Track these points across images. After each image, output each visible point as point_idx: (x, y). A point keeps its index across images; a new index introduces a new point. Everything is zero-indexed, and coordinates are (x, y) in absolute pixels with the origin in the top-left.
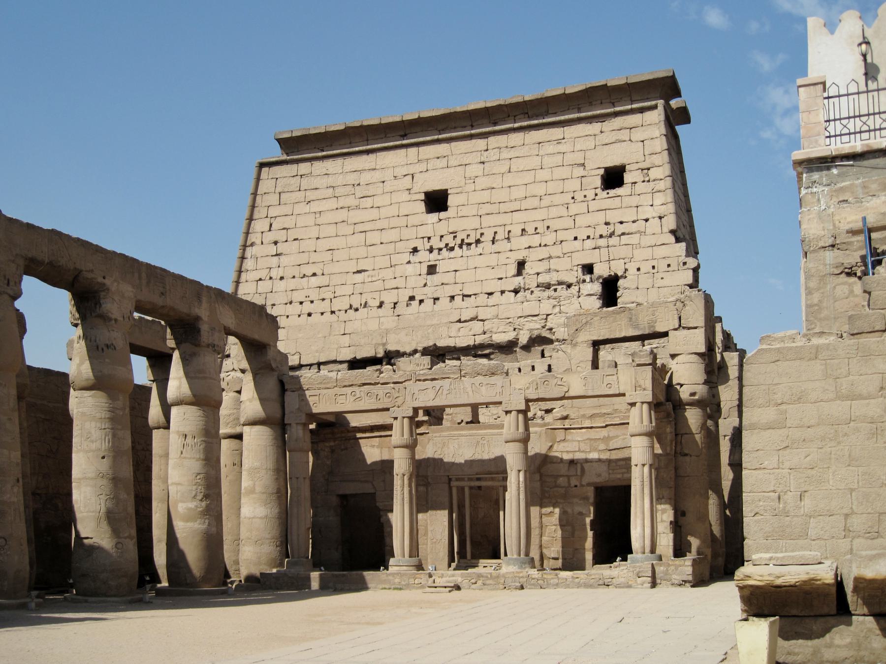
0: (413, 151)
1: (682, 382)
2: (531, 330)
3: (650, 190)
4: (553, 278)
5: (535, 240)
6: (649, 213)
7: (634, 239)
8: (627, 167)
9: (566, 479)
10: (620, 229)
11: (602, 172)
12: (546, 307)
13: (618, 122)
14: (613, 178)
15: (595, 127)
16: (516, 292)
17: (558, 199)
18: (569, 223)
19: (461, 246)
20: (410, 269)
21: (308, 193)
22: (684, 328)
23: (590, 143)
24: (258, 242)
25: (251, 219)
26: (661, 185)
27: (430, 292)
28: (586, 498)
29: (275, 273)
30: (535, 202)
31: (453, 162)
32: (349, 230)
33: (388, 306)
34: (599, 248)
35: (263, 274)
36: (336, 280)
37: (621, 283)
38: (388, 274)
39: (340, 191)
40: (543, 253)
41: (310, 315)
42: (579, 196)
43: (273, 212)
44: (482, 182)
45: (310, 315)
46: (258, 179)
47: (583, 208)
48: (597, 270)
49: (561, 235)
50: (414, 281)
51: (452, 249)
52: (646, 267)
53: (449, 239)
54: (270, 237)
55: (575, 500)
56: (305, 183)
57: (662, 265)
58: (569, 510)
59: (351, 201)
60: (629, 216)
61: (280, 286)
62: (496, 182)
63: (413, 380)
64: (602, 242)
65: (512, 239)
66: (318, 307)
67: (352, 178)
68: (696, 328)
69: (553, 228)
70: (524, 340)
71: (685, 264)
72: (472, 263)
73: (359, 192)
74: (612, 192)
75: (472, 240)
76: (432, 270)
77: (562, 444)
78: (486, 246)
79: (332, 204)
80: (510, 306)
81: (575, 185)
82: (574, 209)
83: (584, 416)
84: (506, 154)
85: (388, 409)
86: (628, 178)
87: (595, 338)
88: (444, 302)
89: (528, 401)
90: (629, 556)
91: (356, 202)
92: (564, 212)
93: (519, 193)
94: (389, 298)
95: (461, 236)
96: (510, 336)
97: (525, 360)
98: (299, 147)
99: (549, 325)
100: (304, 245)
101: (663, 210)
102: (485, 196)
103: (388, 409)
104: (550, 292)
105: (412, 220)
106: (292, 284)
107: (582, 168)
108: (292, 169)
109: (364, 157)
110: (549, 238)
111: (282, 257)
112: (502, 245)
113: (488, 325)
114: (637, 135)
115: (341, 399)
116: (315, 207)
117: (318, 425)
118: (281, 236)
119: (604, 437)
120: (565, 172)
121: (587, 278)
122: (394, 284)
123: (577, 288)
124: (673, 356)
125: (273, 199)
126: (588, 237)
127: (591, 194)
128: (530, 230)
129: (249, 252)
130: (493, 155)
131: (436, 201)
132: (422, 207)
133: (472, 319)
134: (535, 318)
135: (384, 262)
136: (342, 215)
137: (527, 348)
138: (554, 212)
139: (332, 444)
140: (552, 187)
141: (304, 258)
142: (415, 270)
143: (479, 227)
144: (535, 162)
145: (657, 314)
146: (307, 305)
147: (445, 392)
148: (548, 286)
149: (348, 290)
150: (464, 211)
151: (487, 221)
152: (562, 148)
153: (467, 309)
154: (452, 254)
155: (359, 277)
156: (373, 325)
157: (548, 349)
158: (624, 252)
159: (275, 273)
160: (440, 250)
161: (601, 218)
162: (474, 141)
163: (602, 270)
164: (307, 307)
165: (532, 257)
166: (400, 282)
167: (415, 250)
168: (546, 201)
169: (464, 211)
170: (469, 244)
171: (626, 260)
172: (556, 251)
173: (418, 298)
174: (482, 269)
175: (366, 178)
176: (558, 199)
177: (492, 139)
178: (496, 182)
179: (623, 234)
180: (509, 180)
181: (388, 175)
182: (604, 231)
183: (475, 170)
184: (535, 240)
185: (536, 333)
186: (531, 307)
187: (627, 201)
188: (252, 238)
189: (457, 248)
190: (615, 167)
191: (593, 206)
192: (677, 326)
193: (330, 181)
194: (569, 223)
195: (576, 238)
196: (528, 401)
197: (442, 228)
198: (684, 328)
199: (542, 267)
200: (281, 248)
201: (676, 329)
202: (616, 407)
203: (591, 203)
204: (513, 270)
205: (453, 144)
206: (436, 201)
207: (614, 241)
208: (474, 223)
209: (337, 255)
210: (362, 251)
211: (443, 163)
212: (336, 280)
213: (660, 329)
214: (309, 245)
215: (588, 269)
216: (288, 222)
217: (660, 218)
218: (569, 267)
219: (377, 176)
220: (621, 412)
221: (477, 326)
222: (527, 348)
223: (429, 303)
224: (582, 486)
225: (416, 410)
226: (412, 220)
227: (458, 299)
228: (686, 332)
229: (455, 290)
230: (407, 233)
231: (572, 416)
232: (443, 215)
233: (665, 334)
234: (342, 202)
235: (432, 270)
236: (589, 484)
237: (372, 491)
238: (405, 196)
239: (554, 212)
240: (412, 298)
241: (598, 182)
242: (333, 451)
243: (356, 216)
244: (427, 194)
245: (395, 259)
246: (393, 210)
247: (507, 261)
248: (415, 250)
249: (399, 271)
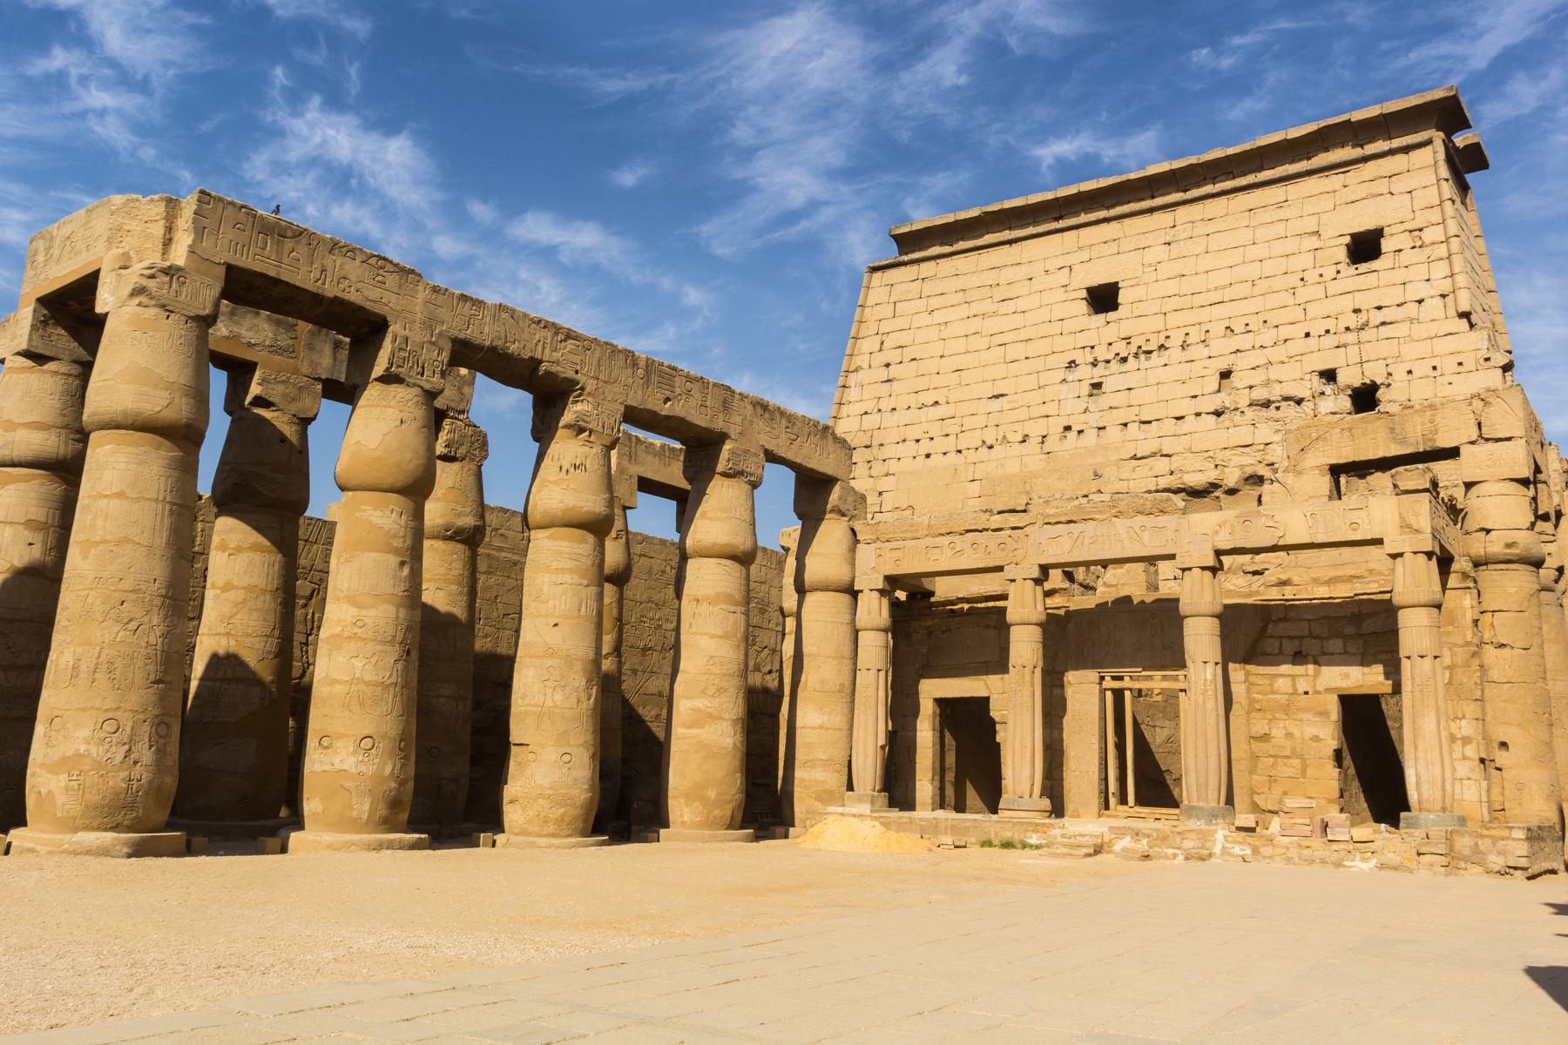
1: (1488, 527)
2: (1242, 467)
3: (1424, 259)
5: (1244, 342)
6: (1423, 291)
7: (1400, 330)
8: (1386, 231)
9: (1289, 680)
11: (1347, 239)
12: (1264, 433)
13: (1371, 168)
14: (1365, 247)
16: (1218, 414)
18: (1298, 314)
19: (1136, 356)
21: (931, 300)
22: (1487, 440)
23: (1327, 203)
24: (865, 365)
27: (1094, 419)
28: (1324, 714)
29: (884, 405)
30: (1244, 289)
31: (1125, 246)
33: (1034, 441)
34: (1345, 346)
35: (868, 406)
36: (965, 409)
37: (1380, 394)
38: (1036, 397)
40: (1258, 358)
41: (928, 456)
42: (1312, 276)
43: (884, 328)
44: (1167, 269)
45: (928, 456)
47: (1319, 292)
48: (1343, 378)
49: (1285, 332)
51: (1124, 360)
52: (1421, 369)
55: (1305, 716)
56: (928, 288)
57: (1449, 365)
58: (1297, 733)
59: (987, 306)
61: (891, 420)
62: (1188, 266)
63: (1040, 523)
64: (1350, 338)
65: (1212, 343)
66: (940, 444)
67: (989, 278)
68: (1509, 439)
69: (1272, 322)
71: (1487, 359)
72: (1153, 377)
73: (999, 294)
74: (1363, 267)
75: (1153, 346)
77: (1282, 625)
78: (1174, 354)
79: (964, 311)
80: (1208, 433)
81: (1306, 261)
82: (1304, 294)
83: (1316, 581)
84: (1201, 229)
85: (1000, 569)
86: (1386, 245)
87: (1334, 461)
88: (1114, 433)
89: (1219, 553)
90: (1402, 815)
91: (995, 307)
92: (1289, 300)
93: (1223, 278)
94: (1035, 430)
95: (1135, 343)
99: (1270, 459)
100: (922, 367)
103: (1000, 569)
104: (1272, 412)
105: (1069, 325)
107: (1315, 238)
108: (910, 271)
111: (895, 384)
112: (1197, 352)
113: (1175, 463)
115: (934, 554)
116: (939, 317)
117: (910, 596)
119: (1353, 614)
120: (1291, 245)
121: (1328, 389)
122: (1043, 410)
123: (1311, 405)
124: (1469, 486)
125: (887, 310)
126: (1328, 332)
127: (1330, 272)
128: (1238, 327)
131: (1103, 299)
132: (1083, 307)
133: (1153, 455)
134: (1247, 450)
135: (1031, 382)
136: (975, 324)
138: (1273, 301)
139: (930, 623)
140: (1269, 267)
141: (922, 383)
143: (1161, 328)
144: (1245, 236)
145: (1438, 419)
146: (925, 443)
147: (1087, 541)
148: (1266, 404)
149: (980, 421)
151: (1174, 320)
154: (1126, 367)
156: (1013, 467)
158: (1387, 349)
159: (885, 405)
160: (1108, 362)
161: (1348, 303)
162: (1156, 215)
163: (1350, 377)
164: (925, 446)
165: (1241, 363)
166: (1051, 409)
167: (1072, 364)
168: (1262, 286)
169: (1141, 309)
170: (1150, 352)
171: (1389, 361)
172: (1275, 354)
173: (1075, 428)
175: (1009, 274)
177: (1181, 210)
178: (1188, 266)
179: (1383, 323)
180: (1206, 262)
181: (1037, 269)
182: (1353, 321)
184: (1244, 342)
185: (1249, 471)
187: (1386, 277)
189: (1131, 359)
190: (1369, 232)
191: (1334, 288)
192: (1474, 436)
195: (1307, 335)
196: (1219, 553)
197: (1112, 333)
198: (1487, 440)
199: (1256, 378)
200: (894, 371)
201: (1473, 443)
202: (1371, 566)
203: (1330, 285)
204: (1214, 382)
205: (1127, 221)
206: (1103, 299)
207: (1364, 335)
208: (1158, 323)
210: (1001, 370)
211: (1113, 247)
212: (965, 409)
213: (1445, 442)
215: (1329, 376)
216: (903, 338)
217: (1443, 296)
218: (1299, 375)
219: (1023, 272)
220: (1381, 574)
221: (1162, 465)
223: (1091, 435)
224: (1318, 692)
225: (1045, 569)
226: (1069, 325)
227: (1133, 427)
228: (1490, 445)
230: (1060, 343)
231: (1296, 579)
232: (1111, 315)
233: (1452, 453)
234: (975, 308)
236: (1328, 690)
237: (985, 694)
238: (1060, 295)
239: (1273, 301)
240: (1068, 428)
241: (1342, 254)
242: (930, 633)
244: (1089, 290)
245: (1045, 378)
246: (1044, 315)
247: (1205, 372)
248: (1072, 364)
249: (1049, 393)
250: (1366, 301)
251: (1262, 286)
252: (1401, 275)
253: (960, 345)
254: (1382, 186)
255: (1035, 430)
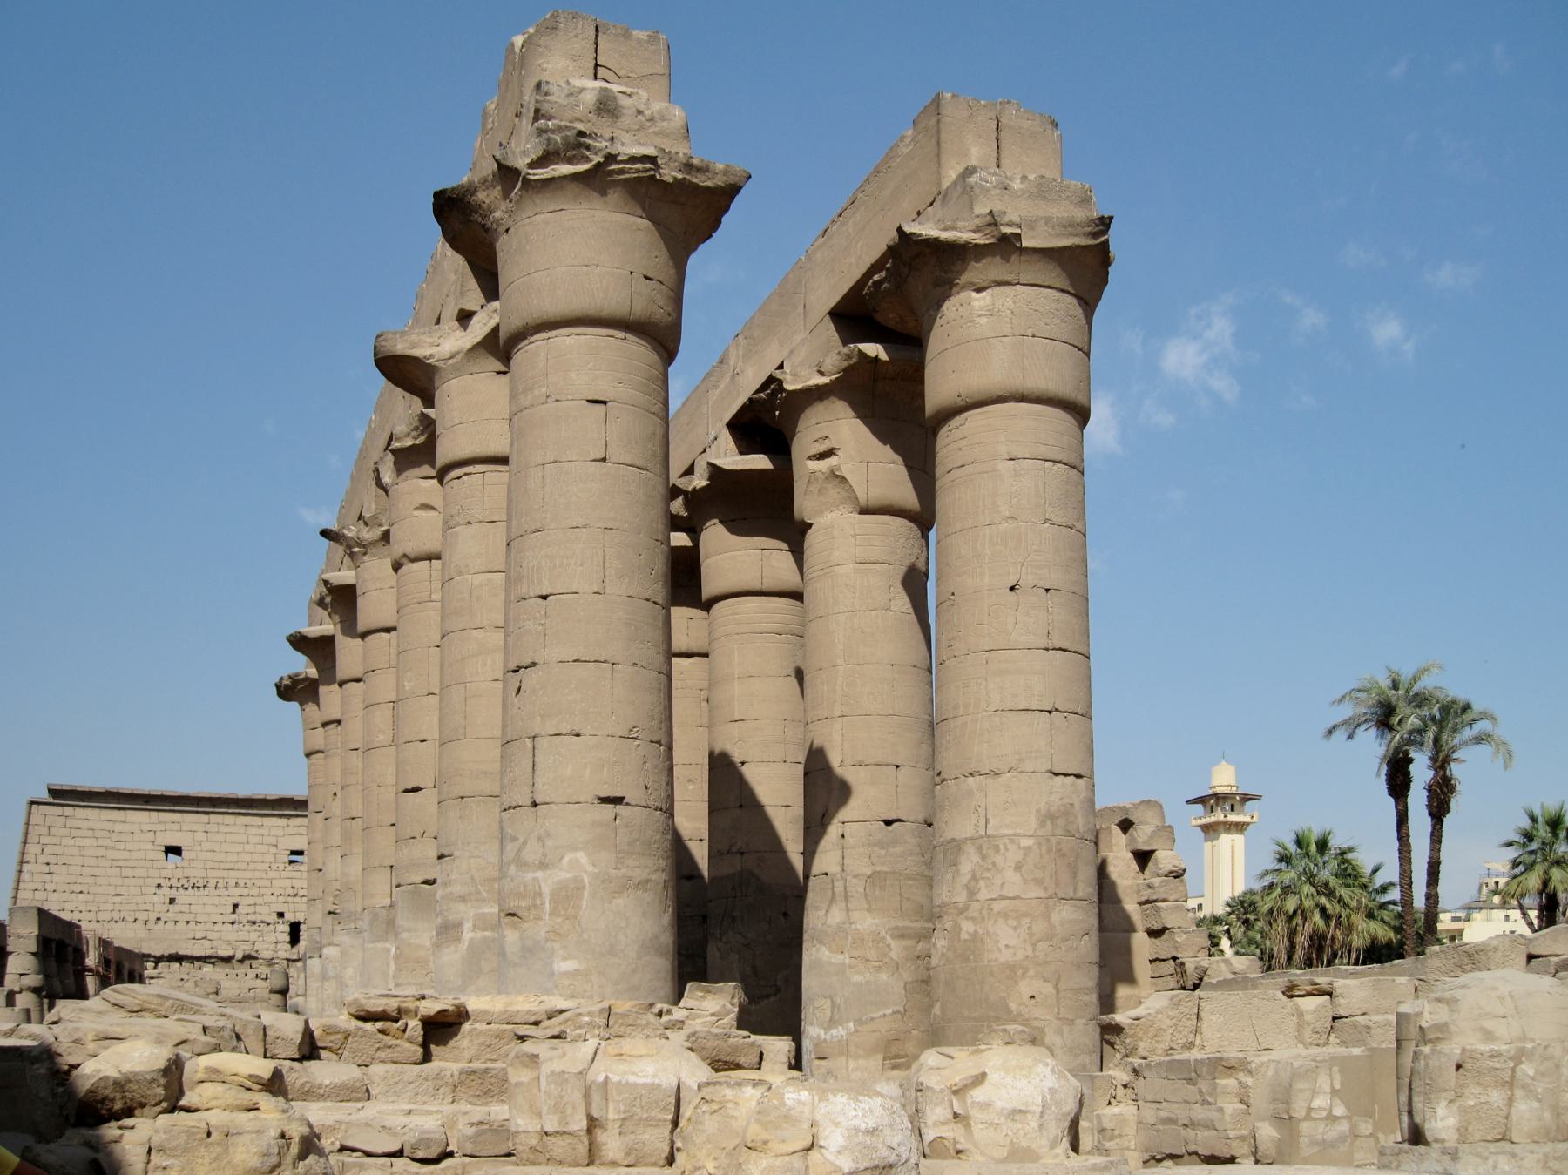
0: (154, 814)
4: (258, 918)
5: (245, 891)
12: (253, 936)
15: (284, 821)
17: (260, 866)
18: (267, 883)
20: (156, 899)
25: (25, 843)
30: (243, 866)
32: (108, 863)
35: (39, 886)
38: (140, 899)
39: (98, 834)
40: (251, 900)
42: (274, 866)
43: (44, 840)
44: (207, 846)
46: (30, 813)
49: (263, 891)
50: (158, 908)
53: (184, 881)
54: (42, 859)
56: (70, 823)
70: (239, 956)
73: (115, 837)
76: (172, 901)
78: (210, 890)
79: (92, 842)
80: (230, 933)
81: (270, 858)
82: (271, 874)
84: (223, 829)
88: (182, 925)
94: (142, 916)
95: (192, 881)
96: (229, 953)
97: (242, 969)
98: (61, 795)
102: (209, 856)
106: (65, 896)
108: (59, 810)
109: (116, 812)
110: (255, 892)
116: (79, 842)
118: (52, 860)
125: (44, 830)
128: (241, 883)
129: (26, 867)
130: (213, 828)
135: (136, 891)
136: (101, 852)
137: (241, 961)
138: (258, 874)
140: (256, 857)
141: (72, 879)
142: (159, 900)
144: (243, 838)
149: (109, 907)
150: (194, 864)
151: (211, 873)
152: (261, 831)
153: (199, 931)
155: (118, 899)
157: (255, 964)
161: (289, 883)
163: (290, 917)
165: (243, 902)
168: (252, 866)
169: (194, 864)
172: (259, 900)
174: (209, 905)
176: (260, 866)
177: (212, 817)
180: (225, 847)
183: (201, 836)
184: (245, 891)
186: (243, 935)
188: (27, 857)
191: (284, 874)
193: (90, 824)
194: (267, 883)
200: (52, 868)
207: (297, 899)
208: (202, 873)
209: (99, 881)
211: (177, 827)
214: (78, 870)
215: (281, 915)
216: (57, 850)
219: (126, 828)
221: (207, 944)
222: (241, 961)
227: (192, 924)
229: (190, 917)
234: (101, 842)
235: (172, 901)
238: (150, 846)
239: (258, 874)
243: (111, 854)
245: (145, 890)
246: (141, 855)
249: (148, 898)
251: (252, 866)
253: (93, 862)
255: (142, 916)
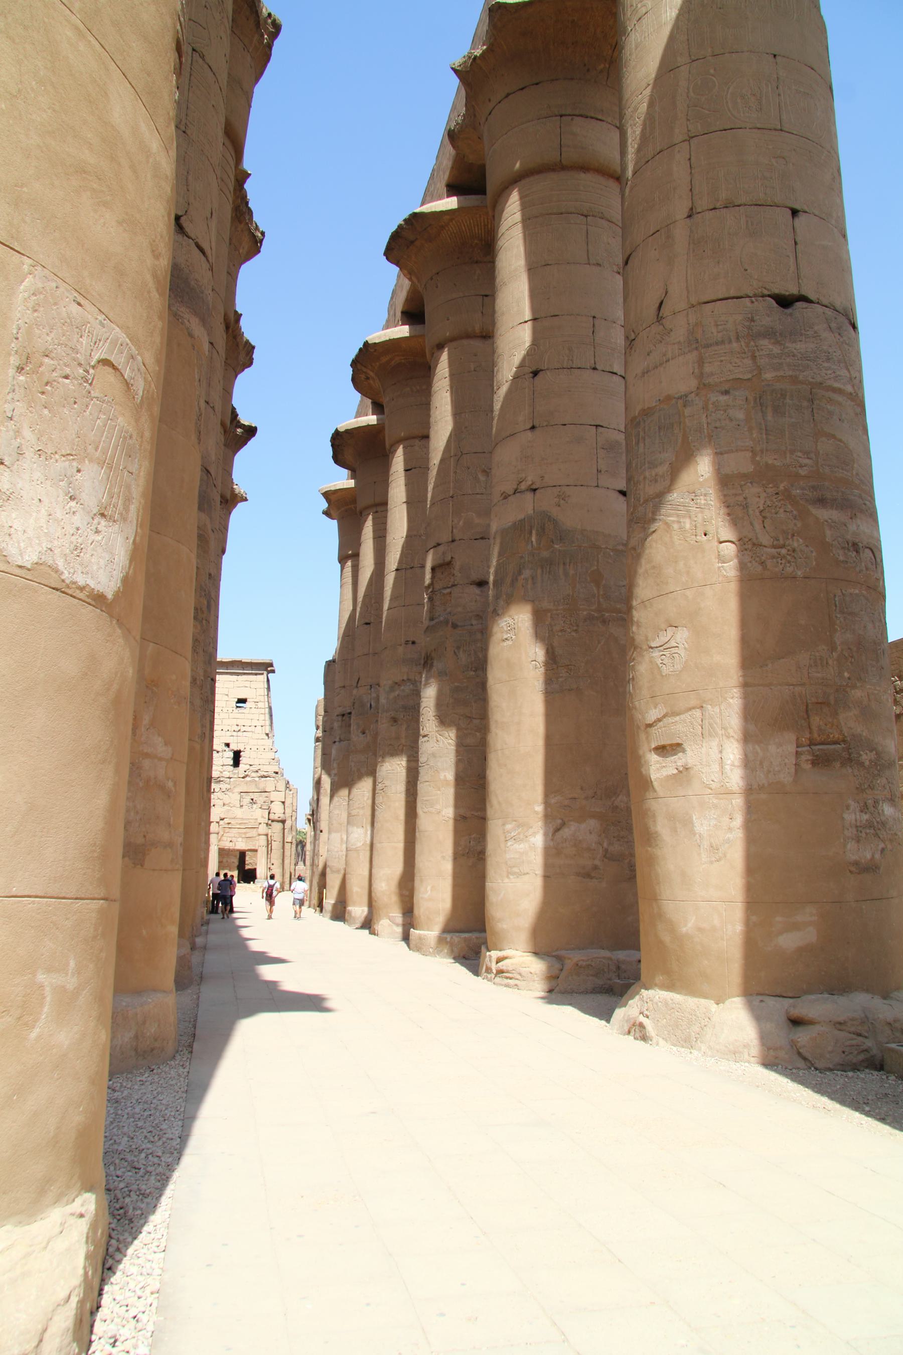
10: (243, 729)
15: (234, 677)
26: (263, 711)
42: (225, 710)
48: (232, 747)
52: (254, 748)
60: (248, 723)
64: (235, 734)
101: (262, 723)
114: (253, 685)
161: (235, 722)
163: (234, 747)
182: (237, 729)
191: (232, 716)
215: (228, 745)
250: (241, 722)
252: (251, 716)
254: (247, 684)
